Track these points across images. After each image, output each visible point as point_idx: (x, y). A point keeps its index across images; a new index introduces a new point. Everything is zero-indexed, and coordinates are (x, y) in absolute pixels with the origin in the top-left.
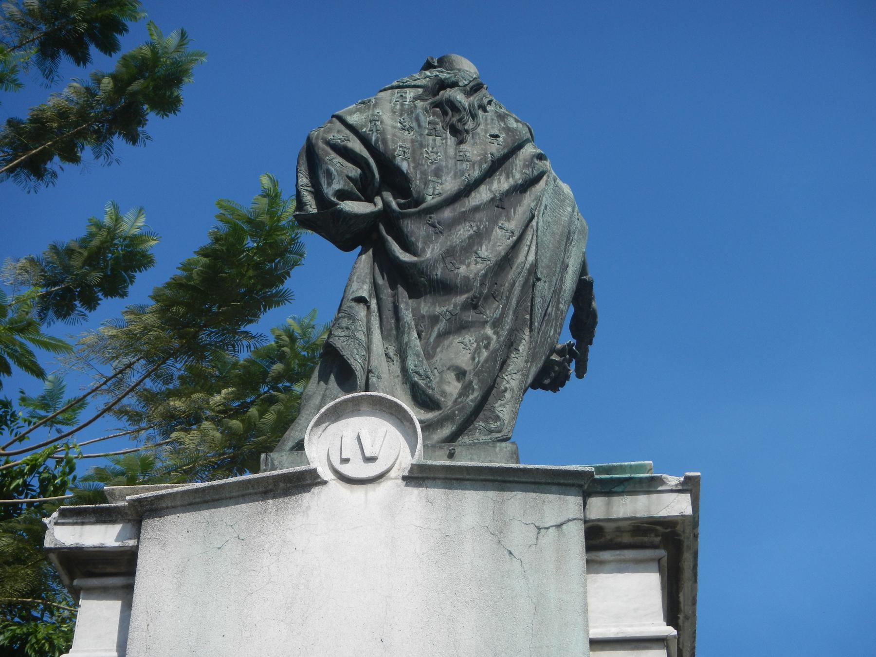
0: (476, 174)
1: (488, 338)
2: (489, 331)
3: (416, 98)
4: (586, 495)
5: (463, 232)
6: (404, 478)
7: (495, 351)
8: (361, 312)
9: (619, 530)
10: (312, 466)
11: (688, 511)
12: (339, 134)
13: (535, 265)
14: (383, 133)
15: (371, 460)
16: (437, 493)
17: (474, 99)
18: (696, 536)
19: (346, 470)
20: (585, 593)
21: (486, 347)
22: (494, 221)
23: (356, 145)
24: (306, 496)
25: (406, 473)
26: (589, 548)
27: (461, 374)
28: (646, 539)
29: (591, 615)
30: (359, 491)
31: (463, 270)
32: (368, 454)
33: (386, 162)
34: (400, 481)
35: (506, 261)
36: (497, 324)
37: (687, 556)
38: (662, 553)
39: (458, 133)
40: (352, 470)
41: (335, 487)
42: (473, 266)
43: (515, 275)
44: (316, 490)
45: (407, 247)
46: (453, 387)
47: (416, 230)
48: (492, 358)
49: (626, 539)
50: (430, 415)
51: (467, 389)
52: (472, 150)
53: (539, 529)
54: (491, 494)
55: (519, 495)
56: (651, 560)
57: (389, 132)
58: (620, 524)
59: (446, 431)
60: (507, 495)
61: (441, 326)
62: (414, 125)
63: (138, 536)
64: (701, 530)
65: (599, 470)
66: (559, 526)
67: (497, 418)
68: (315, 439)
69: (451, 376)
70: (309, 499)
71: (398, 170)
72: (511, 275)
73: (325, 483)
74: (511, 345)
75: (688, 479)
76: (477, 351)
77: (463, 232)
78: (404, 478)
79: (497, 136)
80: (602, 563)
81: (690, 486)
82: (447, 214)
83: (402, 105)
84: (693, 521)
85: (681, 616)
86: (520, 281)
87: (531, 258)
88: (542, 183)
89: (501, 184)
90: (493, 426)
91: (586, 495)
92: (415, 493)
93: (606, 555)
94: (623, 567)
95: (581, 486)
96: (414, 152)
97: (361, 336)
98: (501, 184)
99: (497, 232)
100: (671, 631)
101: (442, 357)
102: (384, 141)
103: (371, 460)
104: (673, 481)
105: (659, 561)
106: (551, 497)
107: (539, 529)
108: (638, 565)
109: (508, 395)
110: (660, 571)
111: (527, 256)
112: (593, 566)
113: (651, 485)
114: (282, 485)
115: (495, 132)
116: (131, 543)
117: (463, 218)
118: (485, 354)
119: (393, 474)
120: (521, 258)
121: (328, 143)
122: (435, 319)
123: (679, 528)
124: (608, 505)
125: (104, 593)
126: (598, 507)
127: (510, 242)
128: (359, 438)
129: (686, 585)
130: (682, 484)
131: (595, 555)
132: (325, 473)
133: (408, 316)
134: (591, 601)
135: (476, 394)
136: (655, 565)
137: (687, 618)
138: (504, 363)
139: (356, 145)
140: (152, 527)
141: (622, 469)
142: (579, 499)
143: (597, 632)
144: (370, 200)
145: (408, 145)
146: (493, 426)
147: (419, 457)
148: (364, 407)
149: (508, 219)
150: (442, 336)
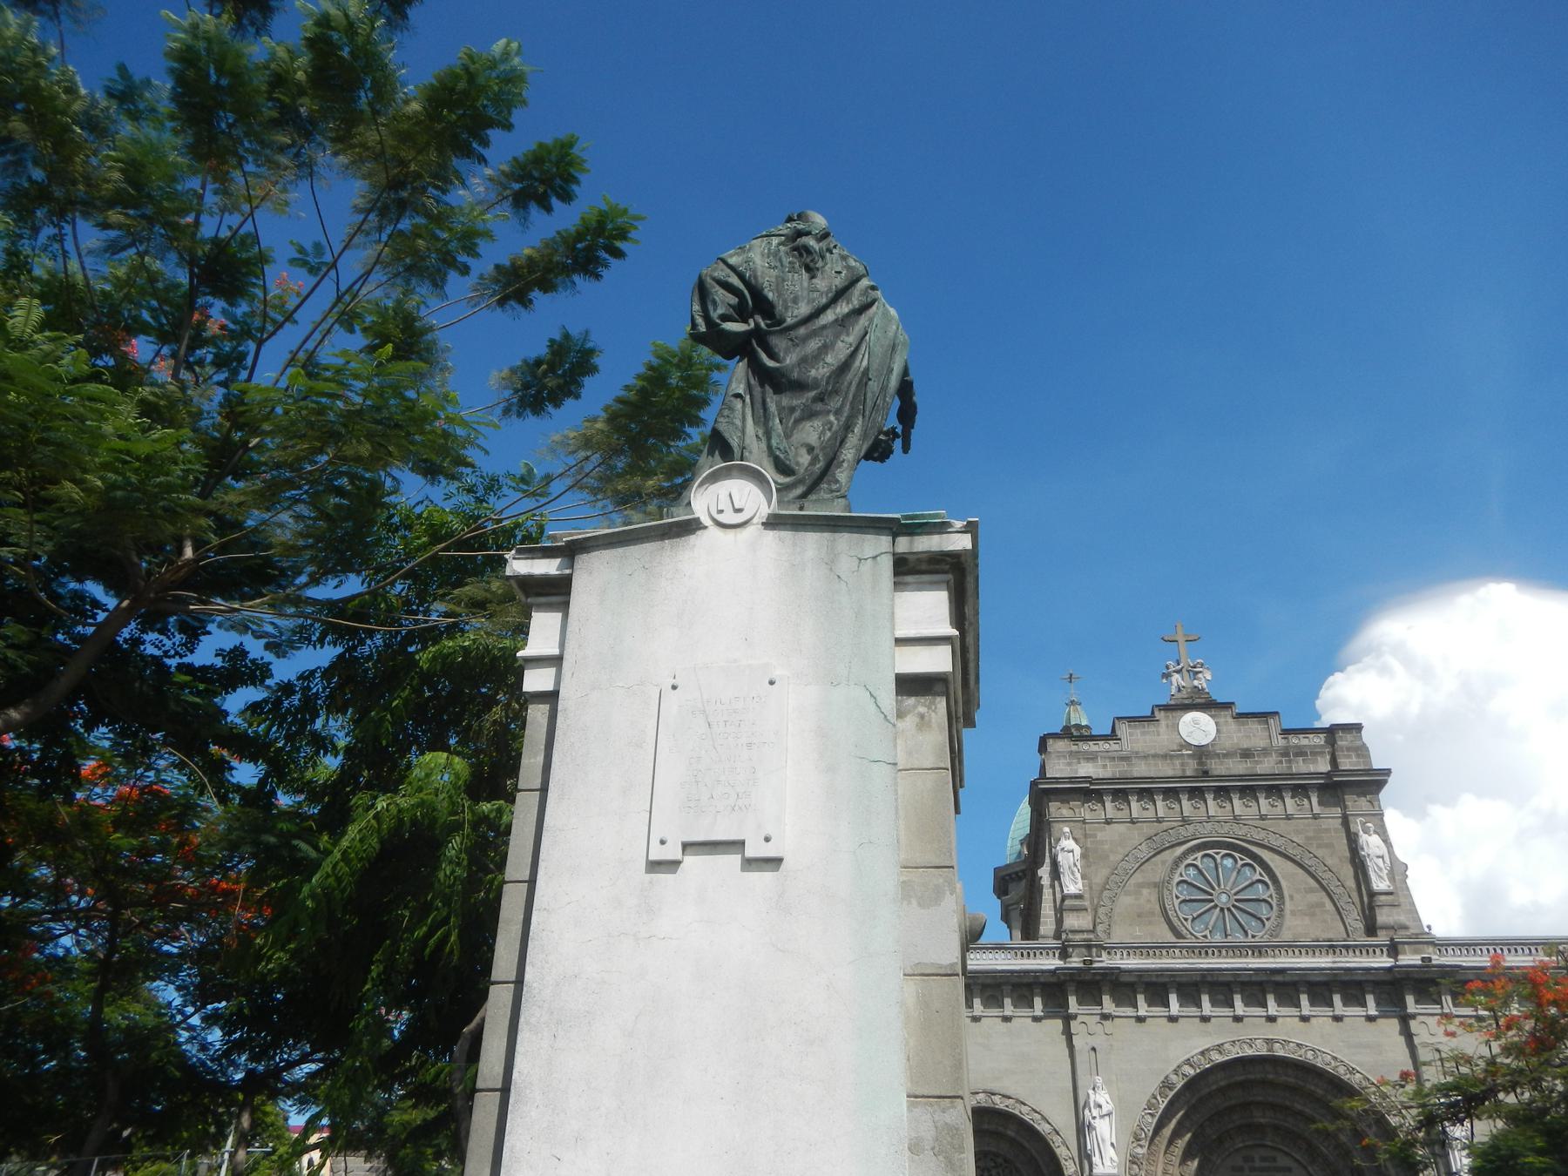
0: (824, 300)
1: (831, 423)
2: (832, 418)
3: (779, 244)
4: (895, 535)
5: (814, 344)
6: (763, 524)
7: (836, 432)
8: (738, 404)
9: (919, 561)
10: (696, 516)
11: (969, 546)
12: (722, 273)
13: (867, 369)
14: (754, 271)
15: (739, 511)
16: (787, 535)
17: (823, 244)
18: (977, 566)
19: (721, 518)
20: (893, 607)
21: (830, 429)
22: (837, 336)
23: (735, 281)
24: (692, 537)
25: (764, 520)
26: (896, 574)
27: (810, 449)
28: (937, 567)
29: (897, 621)
30: (731, 533)
31: (813, 373)
32: (737, 507)
33: (757, 293)
34: (760, 526)
35: (845, 367)
36: (838, 412)
37: (970, 579)
38: (950, 576)
39: (811, 270)
40: (725, 518)
41: (713, 531)
42: (821, 370)
43: (852, 377)
44: (699, 533)
45: (772, 356)
46: (805, 459)
47: (779, 343)
48: (834, 437)
49: (924, 567)
50: (787, 480)
52: (820, 283)
53: (860, 560)
54: (826, 534)
55: (846, 535)
56: (943, 582)
58: (920, 556)
59: (799, 491)
60: (837, 535)
61: (797, 414)
62: (778, 264)
63: (572, 567)
64: (981, 561)
65: (906, 517)
66: (874, 558)
67: (837, 481)
68: (698, 495)
69: (803, 451)
70: (697, 540)
71: (765, 299)
72: (849, 377)
73: (706, 527)
74: (848, 428)
75: (969, 522)
76: (823, 433)
77: (814, 344)
78: (763, 524)
79: (840, 273)
80: (906, 584)
81: (971, 528)
82: (802, 331)
83: (769, 249)
84: (974, 552)
85: (967, 623)
86: (857, 379)
87: (865, 363)
88: (874, 308)
89: (843, 308)
90: (834, 487)
91: (895, 535)
92: (771, 535)
93: (909, 579)
94: (921, 587)
95: (891, 529)
96: (777, 285)
97: (738, 423)
98: (843, 308)
99: (840, 344)
100: (955, 632)
101: (797, 437)
102: (756, 277)
103: (739, 511)
104: (958, 524)
105: (948, 582)
106: (869, 536)
107: (860, 560)
108: (933, 586)
109: (845, 465)
110: (949, 589)
111: (861, 362)
112: (898, 586)
113: (942, 528)
114: (675, 529)
115: (839, 269)
116: (568, 571)
118: (829, 434)
119: (755, 521)
120: (857, 363)
121: (714, 279)
122: (792, 409)
123: (963, 559)
124: (911, 543)
125: (549, 607)
126: (903, 545)
127: (848, 351)
128: (730, 495)
129: (970, 601)
130: (965, 527)
131: (900, 579)
132: (706, 520)
133: (772, 407)
134: (896, 611)
135: (821, 464)
136: (945, 586)
137: (971, 624)
138: (842, 442)
139: (735, 281)
140: (583, 560)
141: (923, 516)
142: (890, 538)
143: (900, 633)
144: (746, 321)
145: (773, 280)
146: (834, 487)
147: (774, 508)
148: (735, 473)
149: (848, 335)
150: (797, 422)
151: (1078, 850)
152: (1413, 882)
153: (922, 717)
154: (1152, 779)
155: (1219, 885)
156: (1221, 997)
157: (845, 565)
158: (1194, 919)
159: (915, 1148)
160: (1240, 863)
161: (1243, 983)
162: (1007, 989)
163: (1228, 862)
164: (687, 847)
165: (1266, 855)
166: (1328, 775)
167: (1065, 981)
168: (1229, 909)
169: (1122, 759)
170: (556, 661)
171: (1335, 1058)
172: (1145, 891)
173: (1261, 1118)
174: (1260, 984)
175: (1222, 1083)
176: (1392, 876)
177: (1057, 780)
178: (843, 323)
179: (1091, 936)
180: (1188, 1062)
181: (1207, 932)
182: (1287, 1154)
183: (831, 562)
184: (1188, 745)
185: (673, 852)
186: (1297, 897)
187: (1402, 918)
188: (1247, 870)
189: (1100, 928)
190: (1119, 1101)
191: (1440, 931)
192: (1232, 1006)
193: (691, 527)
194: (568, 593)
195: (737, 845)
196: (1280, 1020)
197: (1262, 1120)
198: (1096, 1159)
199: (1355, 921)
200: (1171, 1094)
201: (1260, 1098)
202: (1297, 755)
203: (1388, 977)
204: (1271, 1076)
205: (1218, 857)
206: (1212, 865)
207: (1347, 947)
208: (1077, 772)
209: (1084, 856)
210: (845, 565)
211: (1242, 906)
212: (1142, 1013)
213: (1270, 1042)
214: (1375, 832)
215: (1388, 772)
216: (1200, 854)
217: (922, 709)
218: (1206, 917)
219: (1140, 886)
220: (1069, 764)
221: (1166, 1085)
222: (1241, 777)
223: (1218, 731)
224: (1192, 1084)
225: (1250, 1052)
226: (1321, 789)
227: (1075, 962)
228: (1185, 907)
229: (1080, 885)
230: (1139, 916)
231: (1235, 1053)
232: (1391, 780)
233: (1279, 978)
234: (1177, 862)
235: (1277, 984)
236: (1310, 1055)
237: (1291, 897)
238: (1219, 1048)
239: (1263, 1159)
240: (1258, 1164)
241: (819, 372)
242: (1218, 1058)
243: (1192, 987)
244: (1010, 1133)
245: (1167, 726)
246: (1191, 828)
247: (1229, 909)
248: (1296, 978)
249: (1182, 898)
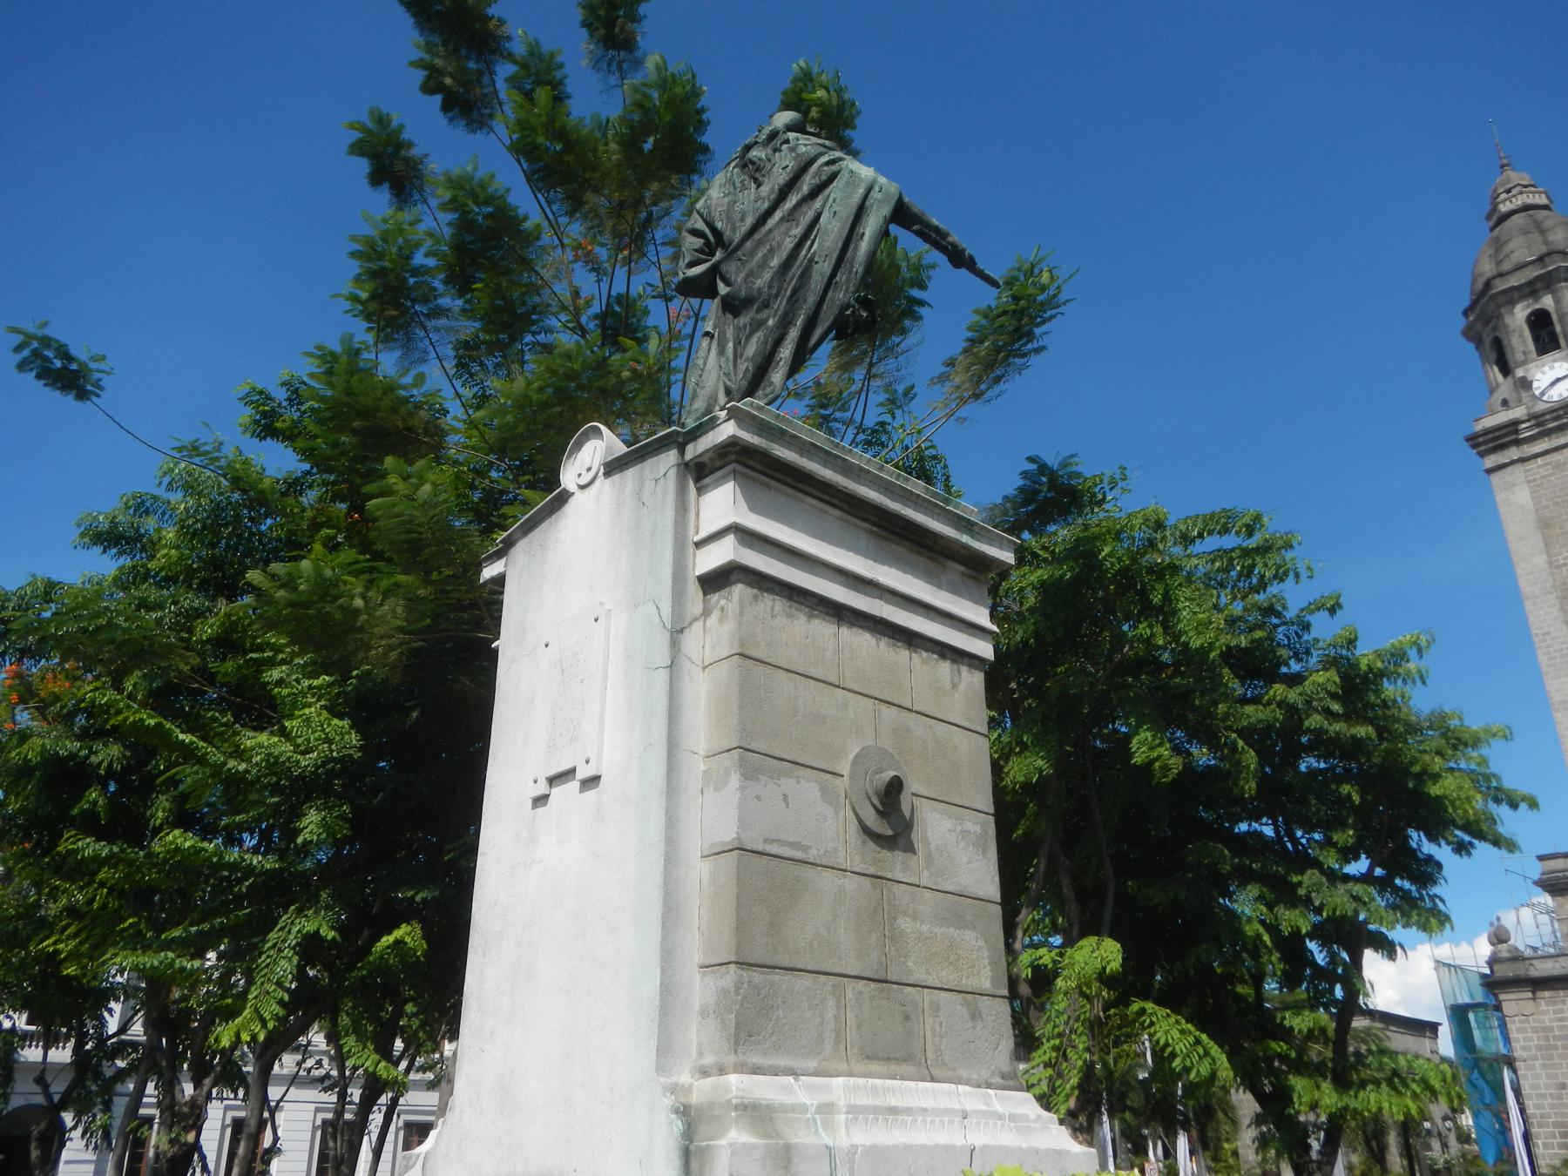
0: (766, 205)
8: (705, 342)
15: (589, 469)
45: (727, 283)
47: (731, 268)
49: (718, 464)
52: (765, 190)
56: (728, 475)
57: (715, 201)
80: (707, 486)
82: (748, 244)
93: (707, 481)
99: (788, 240)
117: (761, 243)
157: (649, 486)
185: (542, 788)
193: (564, 497)
195: (573, 770)
210: (649, 486)
217: (723, 602)
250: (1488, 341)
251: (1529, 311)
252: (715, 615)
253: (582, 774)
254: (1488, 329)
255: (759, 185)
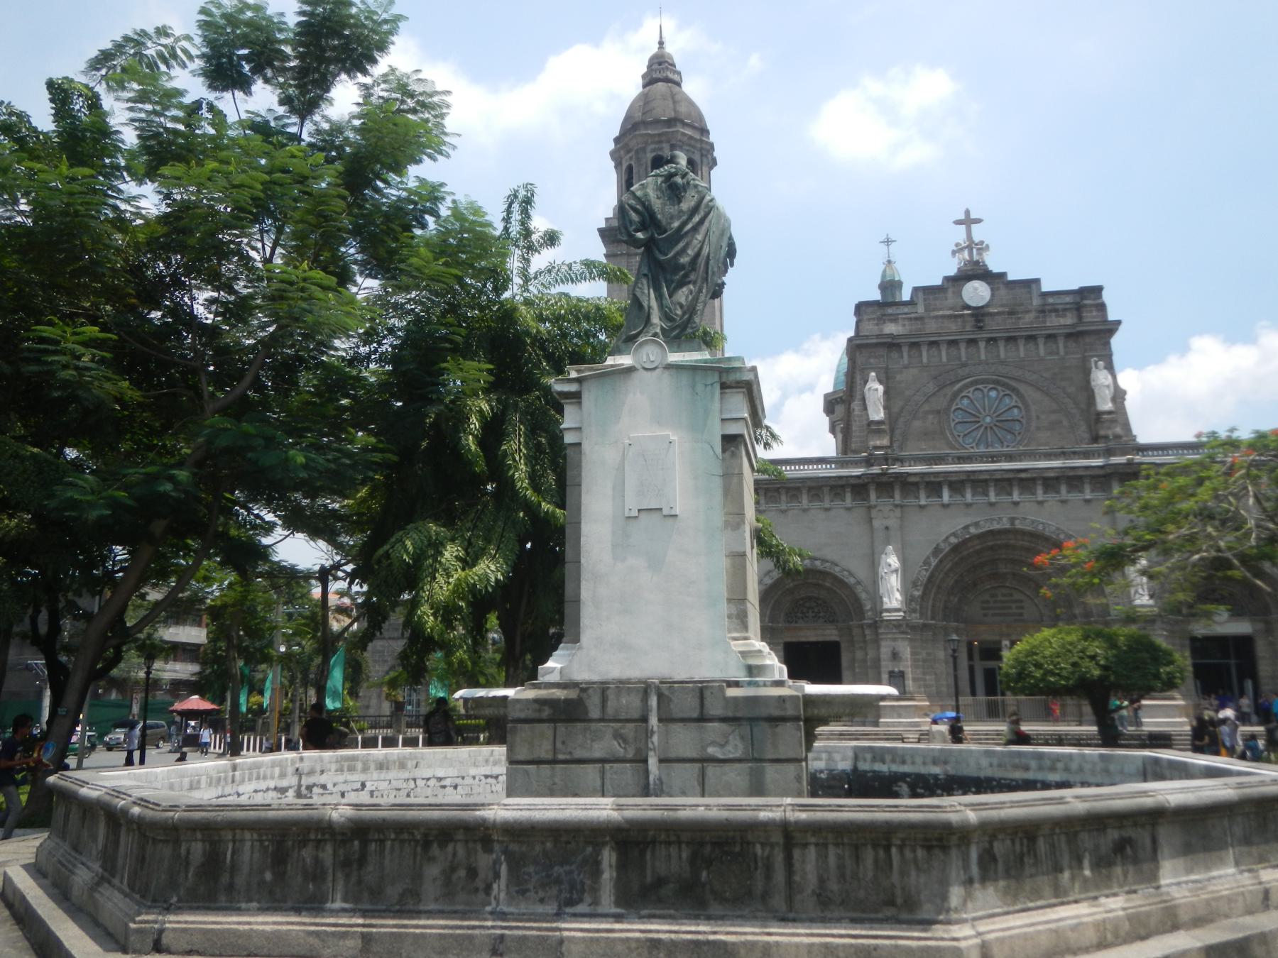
13: (709, 254)
14: (649, 201)
17: (685, 180)
22: (693, 237)
27: (681, 306)
35: (698, 255)
38: (744, 390)
43: (701, 261)
46: (679, 312)
48: (693, 298)
51: (684, 313)
52: (685, 206)
69: (678, 307)
71: (656, 218)
74: (700, 291)
76: (687, 297)
89: (696, 219)
92: (667, 373)
93: (727, 391)
98: (696, 219)
111: (705, 251)
118: (690, 297)
140: (586, 385)
151: (881, 388)
152: (1131, 404)
153: (733, 452)
154: (939, 334)
155: (985, 410)
156: (980, 490)
157: (700, 387)
158: (965, 435)
159: (729, 617)
160: (1002, 394)
161: (997, 480)
162: (826, 490)
163: (993, 394)
164: (639, 510)
165: (1022, 388)
166: (1073, 326)
167: (868, 483)
168: (991, 428)
169: (916, 319)
170: (579, 429)
171: (1058, 529)
172: (930, 417)
173: (1003, 569)
174: (1009, 480)
175: (978, 547)
176: (1114, 400)
177: (867, 337)
178: (695, 229)
179: (889, 451)
180: (954, 534)
181: (974, 445)
182: (1022, 592)
183: (693, 387)
184: (968, 307)
186: (1043, 417)
187: (1118, 430)
188: (1007, 400)
189: (895, 445)
190: (904, 561)
191: (1143, 439)
192: (987, 495)
194: (580, 398)
196: (1021, 504)
197: (1005, 571)
198: (885, 600)
199: (1083, 431)
200: (941, 556)
201: (1003, 556)
202: (1051, 311)
203: (1101, 472)
204: (1012, 542)
205: (985, 390)
206: (981, 396)
207: (1074, 453)
208: (881, 330)
209: (886, 393)
210: (700, 387)
211: (1003, 424)
212: (923, 502)
213: (1012, 520)
214: (1106, 368)
215: (1118, 323)
216: (972, 389)
218: (974, 434)
219: (927, 413)
220: (877, 325)
221: (937, 551)
222: (1007, 330)
223: (993, 295)
224: (955, 549)
225: (996, 526)
226: (1069, 336)
227: (876, 470)
228: (959, 427)
229: (882, 415)
230: (926, 434)
231: (987, 527)
232: (1121, 328)
233: (1023, 475)
234: (955, 395)
235: (1021, 480)
236: (1040, 527)
237: (1038, 417)
238: (976, 524)
239: (1004, 595)
240: (1000, 598)
241: (684, 260)
242: (973, 530)
243: (958, 484)
244: (828, 584)
245: (954, 293)
246: (967, 370)
247: (991, 428)
248: (1035, 475)
249: (957, 420)
250: (625, 166)
251: (653, 154)
252: (728, 454)
253: (665, 512)
254: (628, 157)
255: (680, 201)
